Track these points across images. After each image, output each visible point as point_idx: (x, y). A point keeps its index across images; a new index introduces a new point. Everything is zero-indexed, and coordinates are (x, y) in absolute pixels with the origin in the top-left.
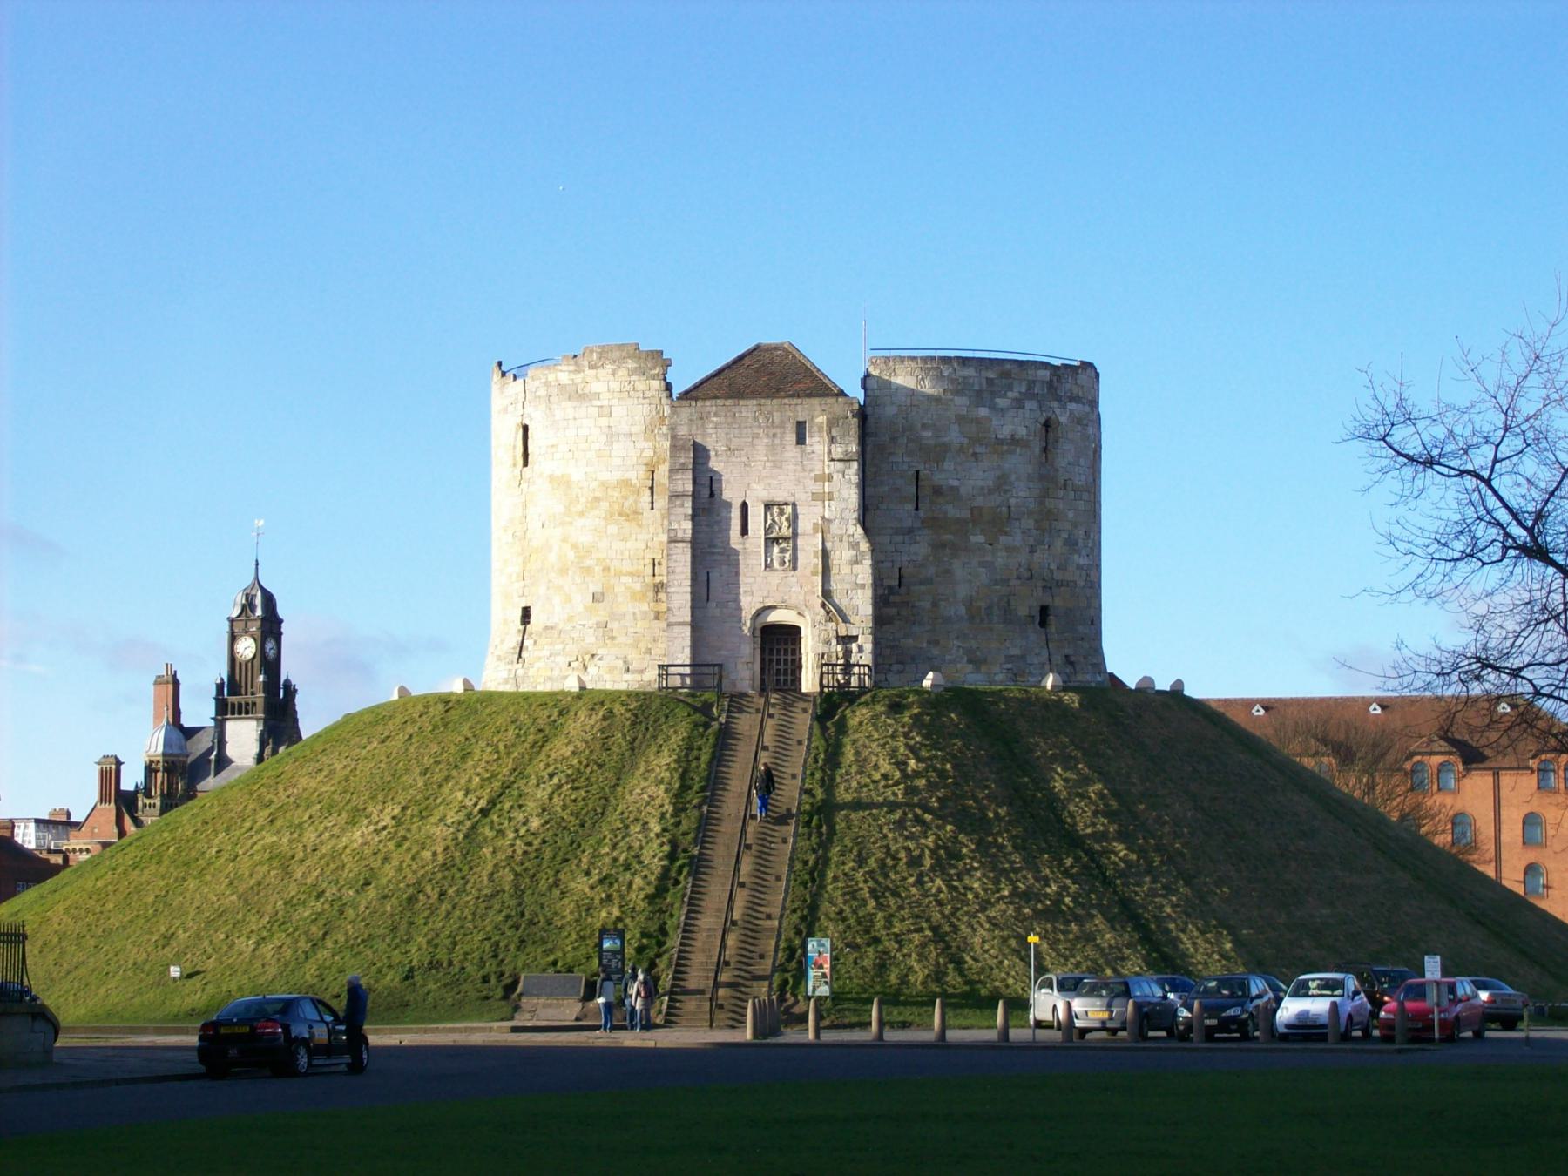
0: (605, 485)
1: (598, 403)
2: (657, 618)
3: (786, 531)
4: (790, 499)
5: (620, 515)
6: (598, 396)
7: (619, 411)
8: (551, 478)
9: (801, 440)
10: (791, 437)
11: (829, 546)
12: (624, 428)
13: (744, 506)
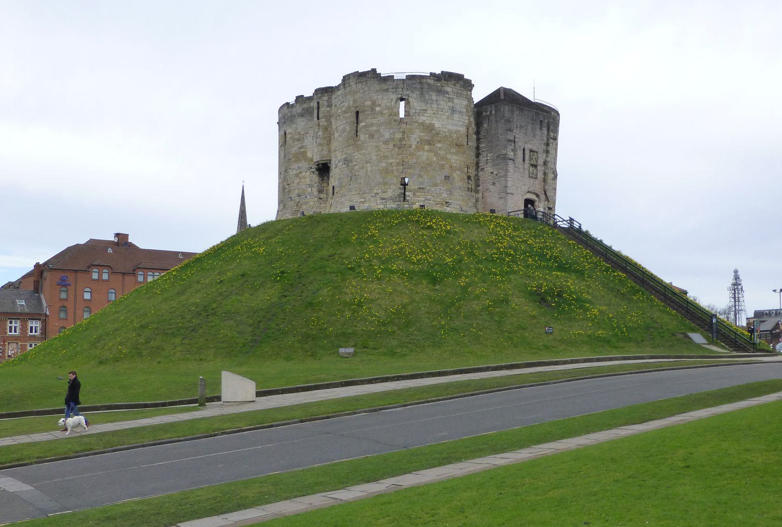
0: (450, 132)
1: (448, 96)
2: (468, 190)
3: (535, 163)
4: (537, 150)
5: (456, 145)
6: (447, 93)
7: (456, 101)
8: (423, 124)
9: (541, 129)
10: (538, 127)
11: (547, 171)
12: (458, 108)
13: (524, 149)
